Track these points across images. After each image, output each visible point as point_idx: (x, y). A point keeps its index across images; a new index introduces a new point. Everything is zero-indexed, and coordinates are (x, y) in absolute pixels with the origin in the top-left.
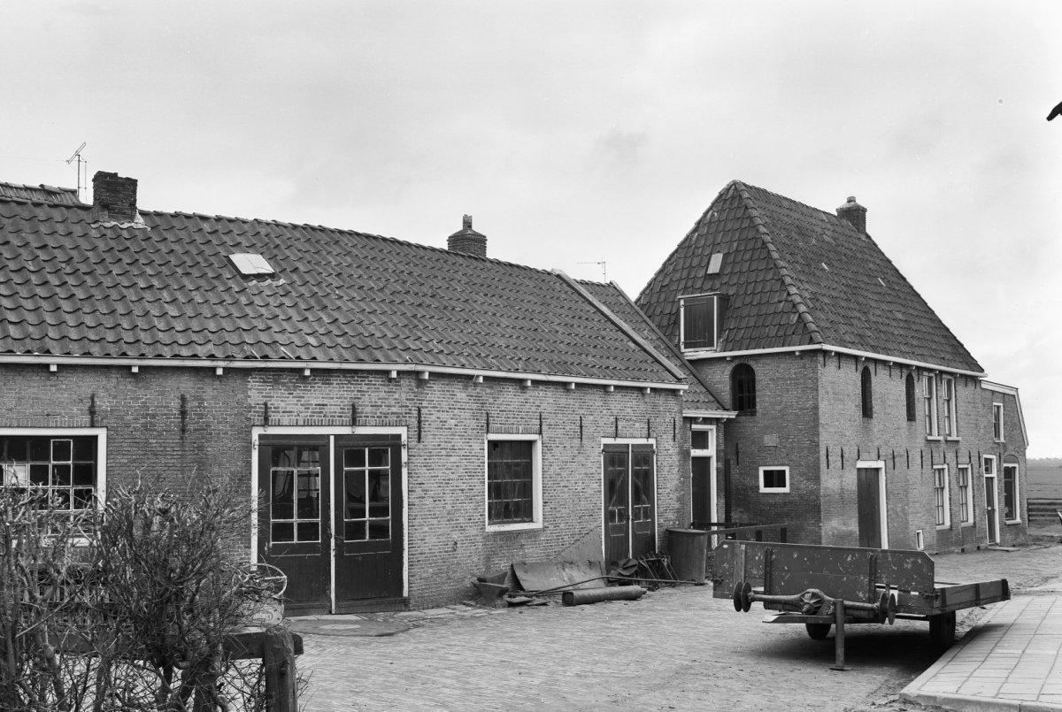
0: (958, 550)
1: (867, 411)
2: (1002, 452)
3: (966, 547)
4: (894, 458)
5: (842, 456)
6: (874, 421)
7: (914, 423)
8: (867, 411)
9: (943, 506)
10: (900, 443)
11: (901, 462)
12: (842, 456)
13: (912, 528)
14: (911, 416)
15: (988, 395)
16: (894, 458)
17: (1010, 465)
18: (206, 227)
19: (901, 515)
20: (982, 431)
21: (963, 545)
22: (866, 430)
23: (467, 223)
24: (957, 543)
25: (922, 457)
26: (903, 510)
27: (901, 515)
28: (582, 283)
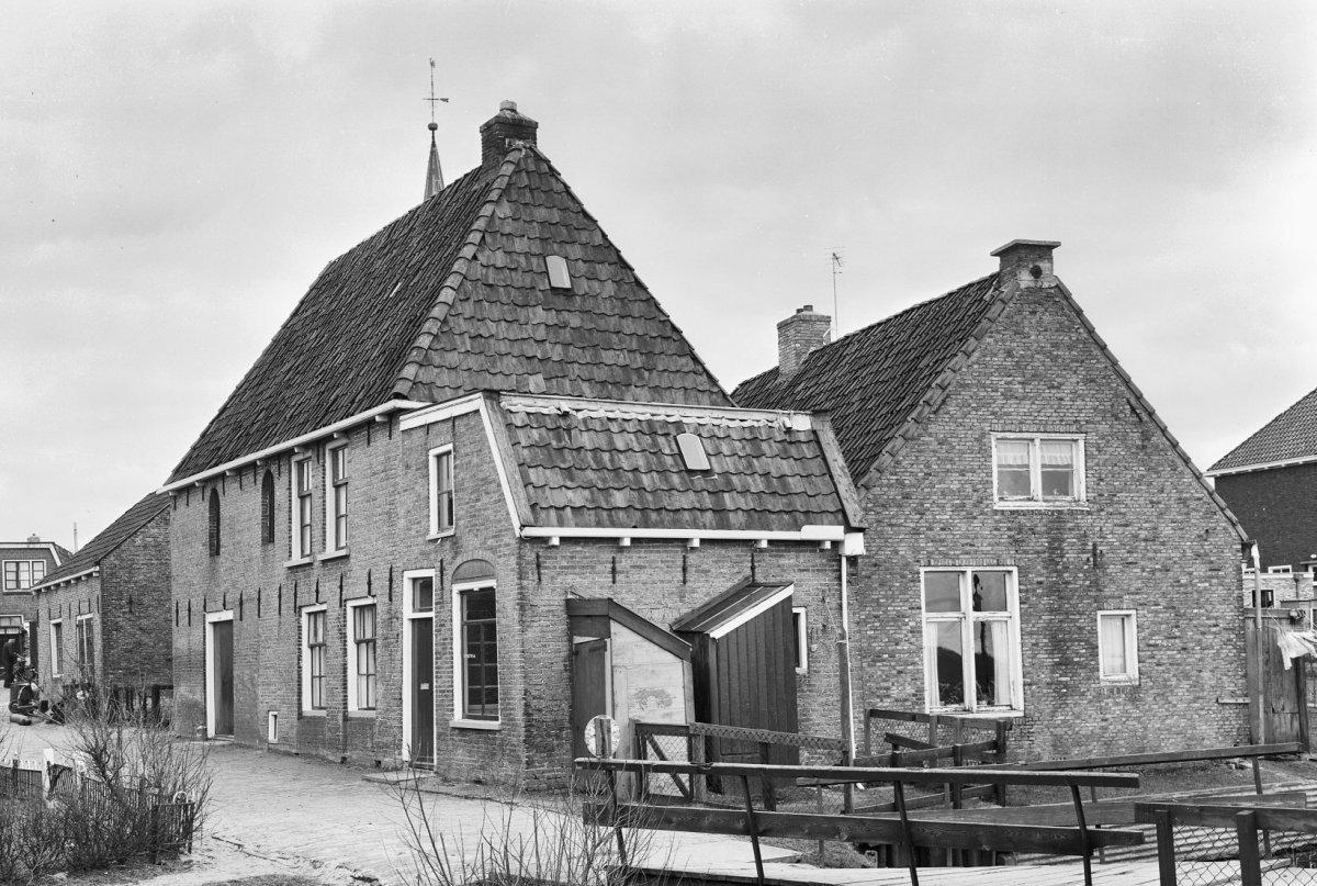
0: (335, 757)
1: (215, 549)
2: (448, 558)
3: (351, 754)
4: (241, 604)
5: (189, 610)
6: (221, 559)
7: (270, 547)
8: (215, 549)
9: (313, 677)
10: (250, 584)
11: (250, 608)
12: (189, 610)
13: (262, 707)
14: (269, 537)
15: (418, 437)
16: (241, 604)
17: (476, 586)
18: (1157, 439)
19: (249, 686)
20: (402, 523)
21: (345, 750)
22: (213, 572)
23: (509, 133)
24: (332, 745)
25: (280, 597)
26: (252, 679)
27: (249, 686)
28: (179, 472)
